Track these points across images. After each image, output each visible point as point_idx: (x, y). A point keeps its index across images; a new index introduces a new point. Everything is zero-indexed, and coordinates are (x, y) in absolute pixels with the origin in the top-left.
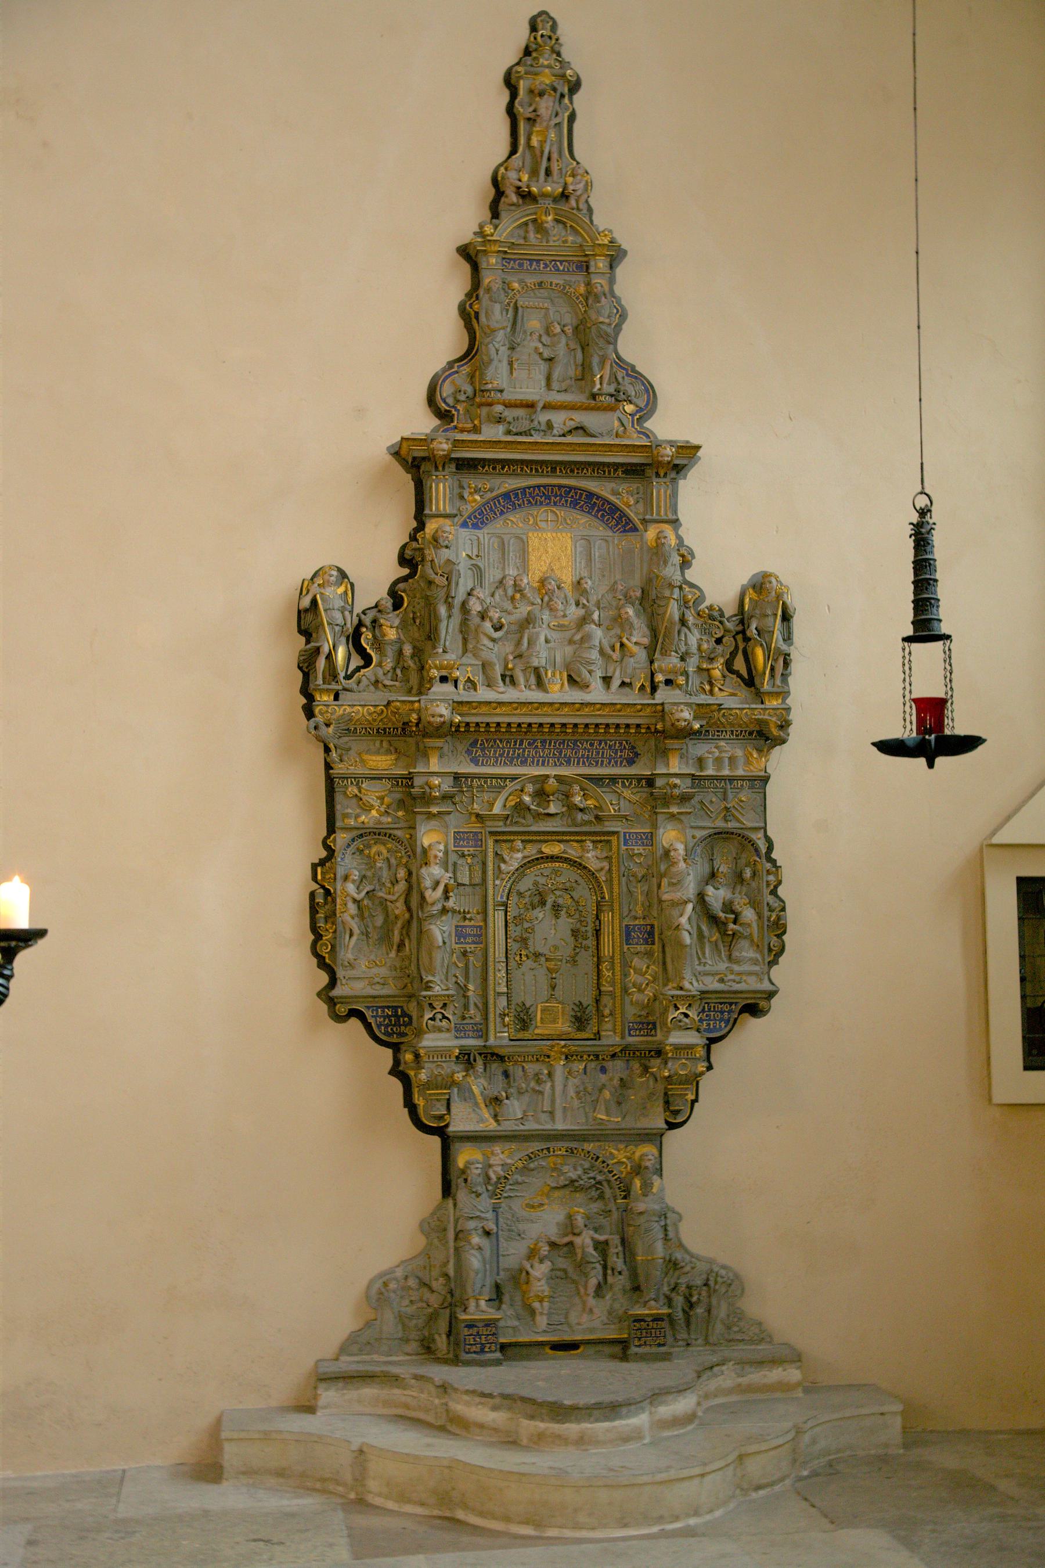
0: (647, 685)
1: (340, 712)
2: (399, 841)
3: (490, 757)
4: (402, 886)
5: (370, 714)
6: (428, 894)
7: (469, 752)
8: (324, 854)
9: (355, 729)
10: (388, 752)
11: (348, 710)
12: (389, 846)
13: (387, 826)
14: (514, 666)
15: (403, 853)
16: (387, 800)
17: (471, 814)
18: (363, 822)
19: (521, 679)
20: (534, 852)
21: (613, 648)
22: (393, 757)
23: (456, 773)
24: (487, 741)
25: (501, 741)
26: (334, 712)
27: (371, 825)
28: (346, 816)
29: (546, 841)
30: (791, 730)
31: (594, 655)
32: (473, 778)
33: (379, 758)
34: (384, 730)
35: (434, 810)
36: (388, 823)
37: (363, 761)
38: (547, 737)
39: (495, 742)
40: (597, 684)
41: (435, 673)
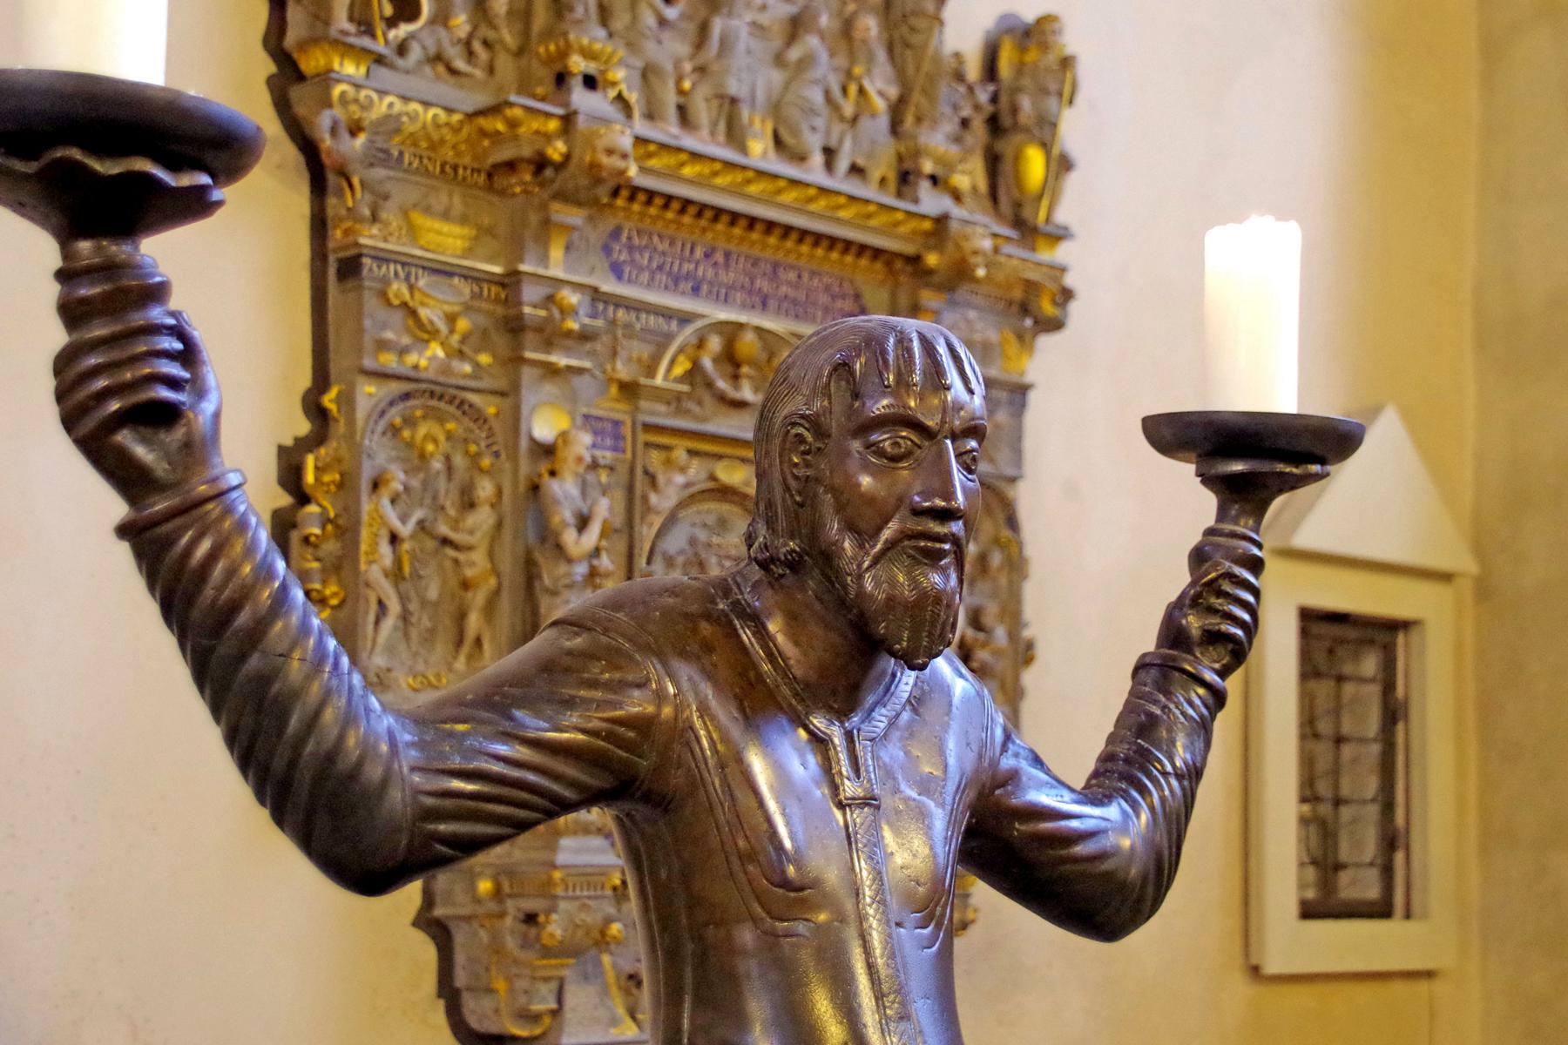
0: (892, 177)
1: (382, 107)
2: (479, 418)
3: (641, 269)
4: (482, 518)
5: (437, 126)
6: (569, 537)
7: (607, 250)
8: (303, 427)
9: (401, 154)
10: (463, 220)
11: (398, 106)
12: (451, 426)
13: (462, 382)
14: (694, 85)
15: (483, 444)
16: (463, 324)
17: (611, 380)
18: (416, 367)
19: (702, 110)
20: (703, 475)
21: (844, 90)
22: (466, 231)
23: (596, 290)
24: (639, 232)
25: (661, 237)
26: (367, 106)
27: (430, 375)
28: (382, 345)
29: (720, 457)
30: (1074, 307)
31: (817, 96)
32: (617, 306)
33: (446, 227)
34: (455, 168)
35: (560, 360)
36: (466, 376)
37: (413, 231)
38: (732, 247)
39: (650, 238)
40: (817, 159)
41: (578, 64)
